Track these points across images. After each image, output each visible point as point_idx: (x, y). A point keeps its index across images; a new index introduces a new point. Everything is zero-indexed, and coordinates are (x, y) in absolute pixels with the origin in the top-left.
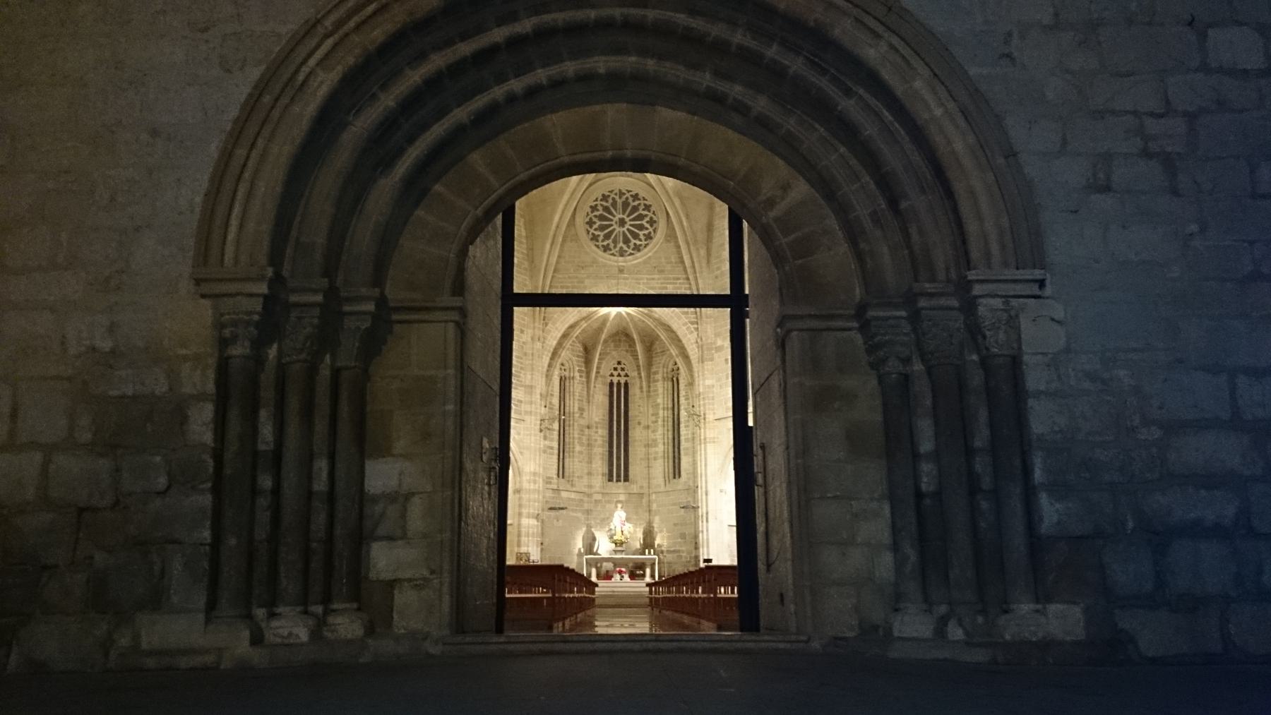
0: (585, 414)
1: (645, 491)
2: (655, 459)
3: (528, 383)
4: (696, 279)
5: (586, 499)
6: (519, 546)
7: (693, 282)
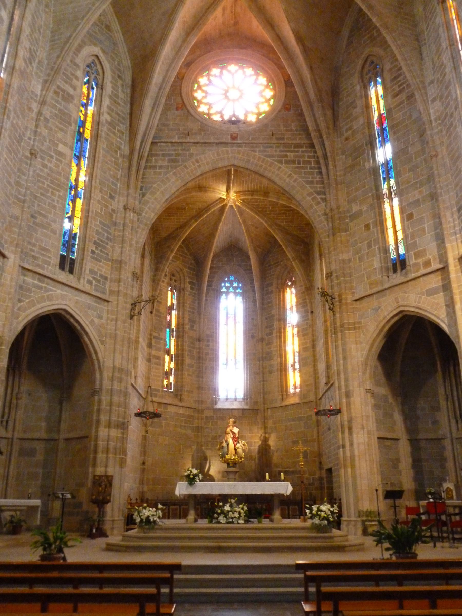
1: (261, 407)
2: (271, 372)
3: (116, 257)
4: (323, 143)
5: (196, 415)
6: (94, 465)
7: (317, 147)
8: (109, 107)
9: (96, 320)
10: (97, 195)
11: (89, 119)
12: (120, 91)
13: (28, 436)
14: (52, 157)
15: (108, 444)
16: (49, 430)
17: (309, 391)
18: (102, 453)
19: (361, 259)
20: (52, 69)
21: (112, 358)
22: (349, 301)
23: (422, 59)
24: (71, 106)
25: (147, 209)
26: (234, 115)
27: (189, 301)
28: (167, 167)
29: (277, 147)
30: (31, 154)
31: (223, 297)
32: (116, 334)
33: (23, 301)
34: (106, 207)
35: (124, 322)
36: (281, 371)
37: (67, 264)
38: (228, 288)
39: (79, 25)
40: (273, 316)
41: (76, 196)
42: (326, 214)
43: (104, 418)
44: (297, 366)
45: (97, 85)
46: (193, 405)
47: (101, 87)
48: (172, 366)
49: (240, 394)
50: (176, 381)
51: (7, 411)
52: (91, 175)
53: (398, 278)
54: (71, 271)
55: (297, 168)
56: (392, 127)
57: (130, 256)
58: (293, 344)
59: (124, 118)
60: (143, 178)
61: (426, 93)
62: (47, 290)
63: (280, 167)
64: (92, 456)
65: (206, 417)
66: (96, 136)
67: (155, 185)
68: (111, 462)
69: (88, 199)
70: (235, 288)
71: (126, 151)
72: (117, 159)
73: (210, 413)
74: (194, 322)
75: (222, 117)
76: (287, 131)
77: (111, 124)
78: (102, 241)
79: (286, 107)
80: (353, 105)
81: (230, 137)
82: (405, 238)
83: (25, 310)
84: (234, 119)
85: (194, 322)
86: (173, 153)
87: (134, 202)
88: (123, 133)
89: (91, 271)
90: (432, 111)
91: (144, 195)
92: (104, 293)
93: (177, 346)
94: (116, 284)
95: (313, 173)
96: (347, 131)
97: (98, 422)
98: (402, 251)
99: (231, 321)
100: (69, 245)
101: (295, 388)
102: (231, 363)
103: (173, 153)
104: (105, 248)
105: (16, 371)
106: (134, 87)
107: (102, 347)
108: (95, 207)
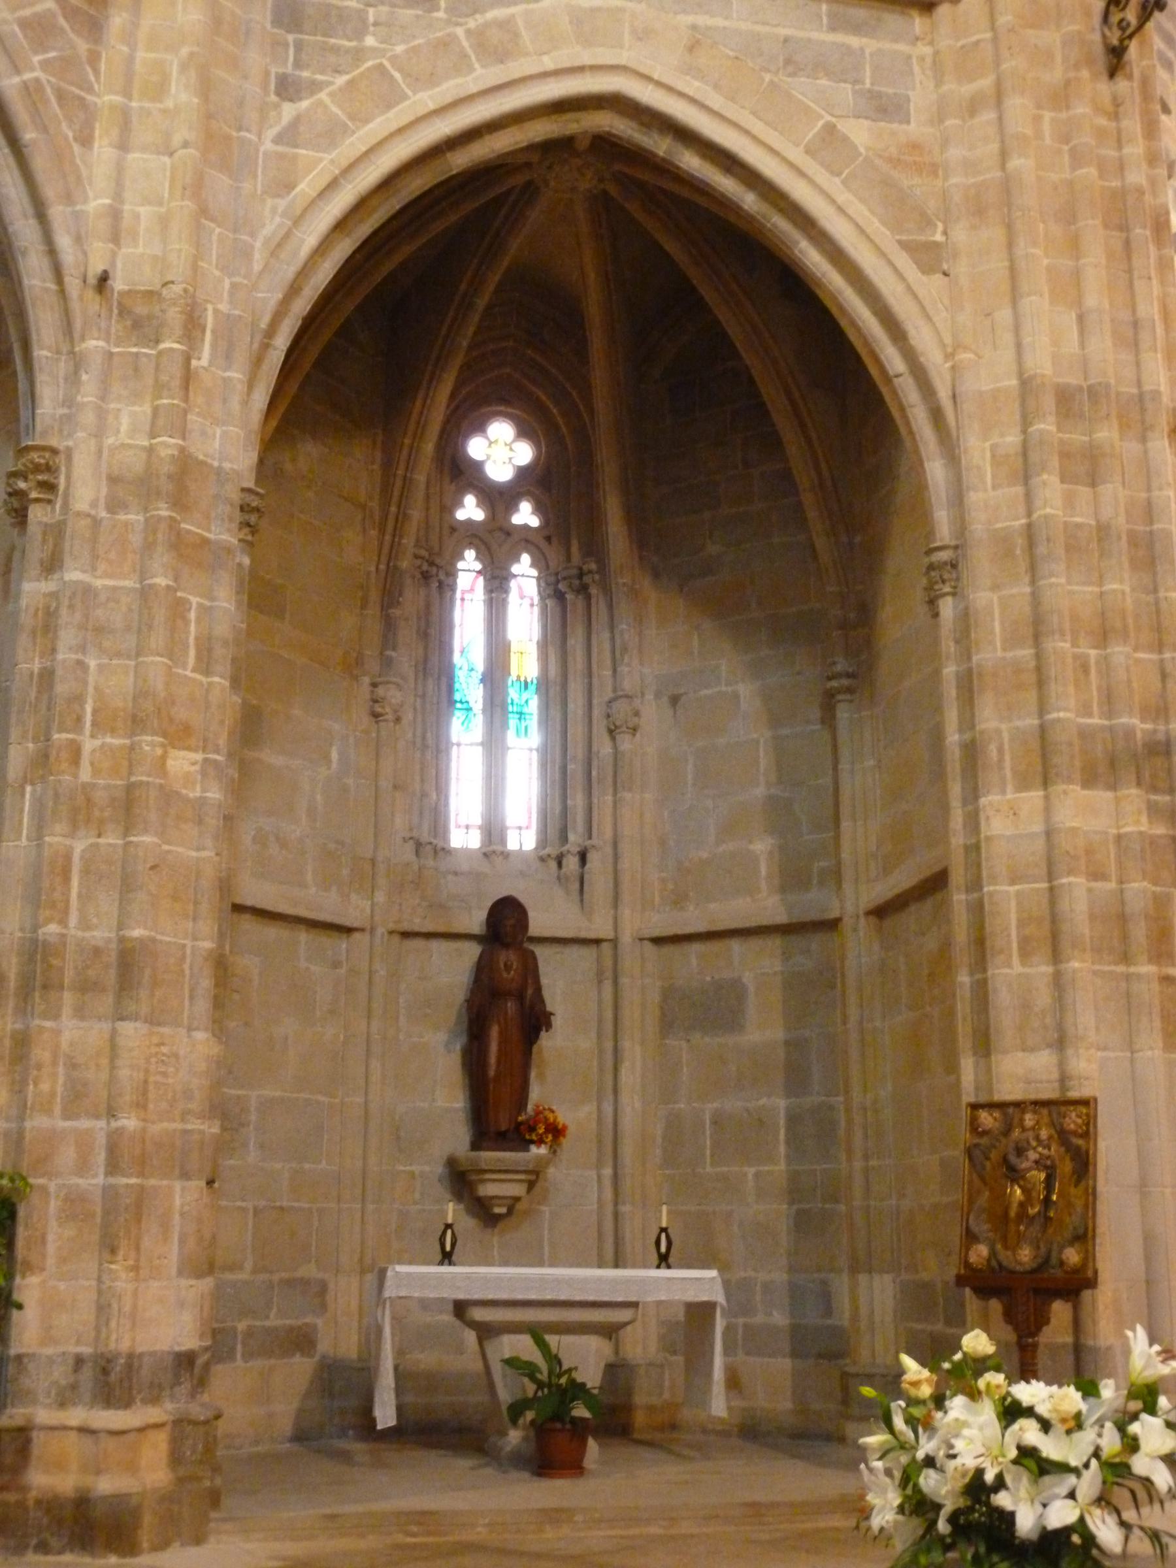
6: (984, 1045)
13: (693, 920)
15: (1053, 893)
16: (792, 877)
18: (1025, 954)
21: (1008, 338)
32: (1007, 186)
33: (315, 87)
35: (1060, 97)
43: (1002, 724)
51: (577, 801)
68: (1084, 1019)
83: (332, 134)
97: (972, 751)
105: (593, 591)
107: (930, 286)
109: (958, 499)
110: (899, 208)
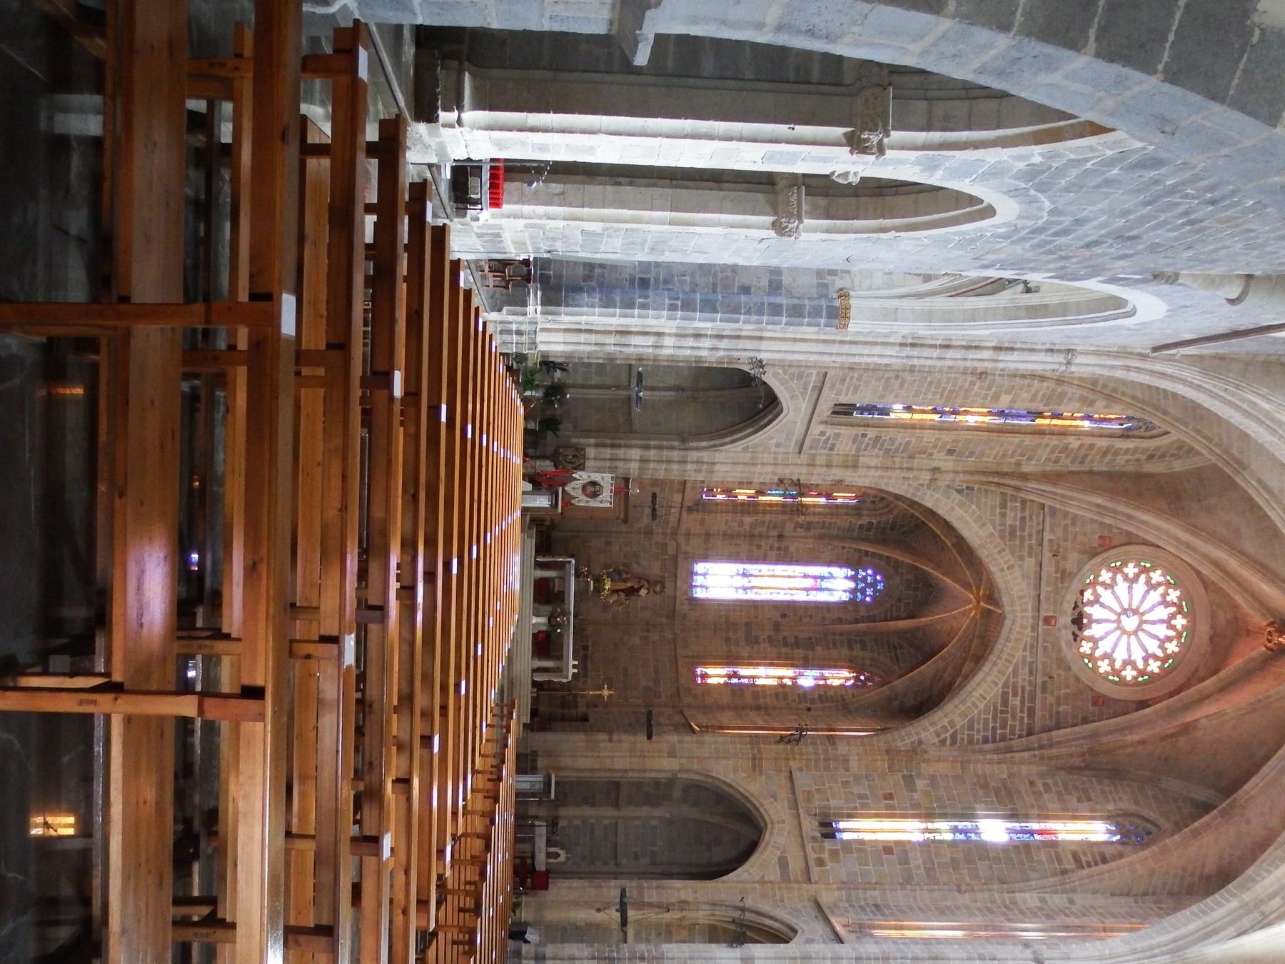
0: (801, 532)
2: (728, 640)
6: (597, 445)
8: (1091, 447)
9: (774, 441)
10: (947, 437)
11: (1068, 422)
12: (1127, 457)
14: (989, 388)
17: (695, 696)
19: (846, 784)
20: (1115, 390)
22: (791, 763)
23: (1113, 894)
24: (1078, 405)
25: (937, 496)
26: (1091, 621)
27: (843, 522)
28: (1003, 524)
29: (1030, 682)
30: (981, 374)
31: (851, 573)
32: (755, 464)
34: (935, 447)
36: (728, 657)
37: (844, 411)
38: (864, 579)
39: (1185, 424)
40: (813, 649)
41: (942, 413)
42: (920, 742)
43: (652, 454)
44: (734, 681)
45: (1128, 429)
46: (684, 527)
47: (1125, 435)
48: (740, 497)
49: (699, 594)
50: (717, 503)
52: (977, 429)
53: (811, 827)
54: (834, 413)
55: (995, 709)
56: (1027, 846)
57: (866, 477)
58: (768, 677)
59: (1082, 462)
60: (986, 491)
61: (1056, 892)
62: (803, 394)
63: (996, 684)
64: (608, 441)
65: (666, 545)
66: (1040, 432)
67: (974, 507)
69: (941, 428)
70: (863, 591)
71: (1026, 468)
72: (1012, 456)
73: (671, 550)
74: (808, 529)
75: (1091, 603)
76: (1058, 698)
77: (1065, 449)
78: (882, 444)
79: (1100, 701)
80: (1086, 797)
81: (1051, 614)
82: (862, 842)
84: (1085, 621)
85: (808, 529)
86: (1026, 533)
87: (944, 480)
88: (1056, 462)
89: (838, 435)
90: (1027, 895)
91: (959, 492)
92: (811, 448)
93: (771, 505)
94: (824, 462)
95: (986, 729)
96: (1046, 785)
97: (647, 447)
98: (846, 836)
99: (809, 583)
100: (871, 409)
101: (704, 676)
102: (745, 582)
103: (1026, 533)
104: (874, 447)
106: (1139, 477)
107: (739, 449)
108: (929, 436)
109: (697, 449)
110: (756, 446)
